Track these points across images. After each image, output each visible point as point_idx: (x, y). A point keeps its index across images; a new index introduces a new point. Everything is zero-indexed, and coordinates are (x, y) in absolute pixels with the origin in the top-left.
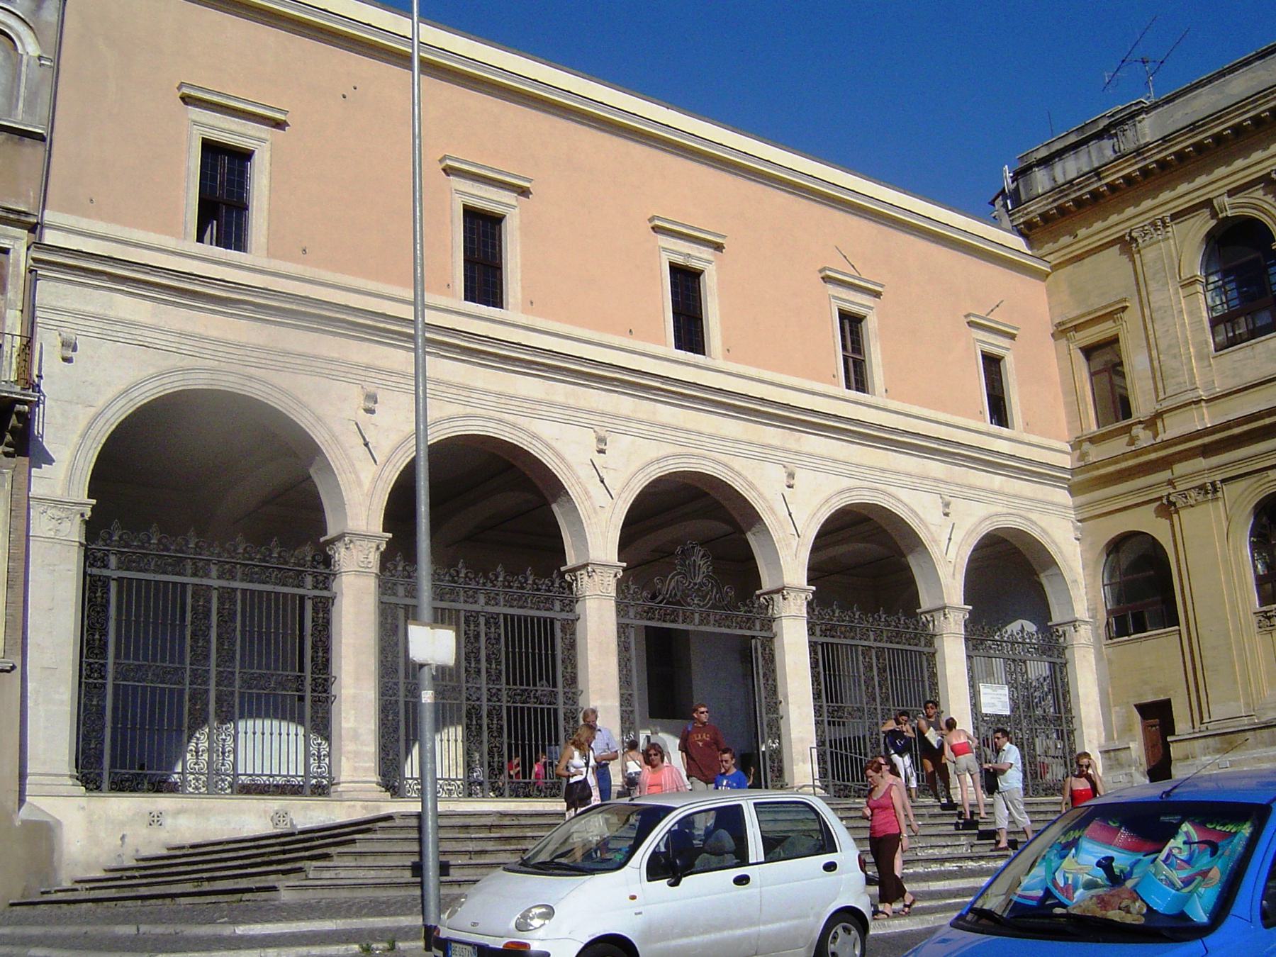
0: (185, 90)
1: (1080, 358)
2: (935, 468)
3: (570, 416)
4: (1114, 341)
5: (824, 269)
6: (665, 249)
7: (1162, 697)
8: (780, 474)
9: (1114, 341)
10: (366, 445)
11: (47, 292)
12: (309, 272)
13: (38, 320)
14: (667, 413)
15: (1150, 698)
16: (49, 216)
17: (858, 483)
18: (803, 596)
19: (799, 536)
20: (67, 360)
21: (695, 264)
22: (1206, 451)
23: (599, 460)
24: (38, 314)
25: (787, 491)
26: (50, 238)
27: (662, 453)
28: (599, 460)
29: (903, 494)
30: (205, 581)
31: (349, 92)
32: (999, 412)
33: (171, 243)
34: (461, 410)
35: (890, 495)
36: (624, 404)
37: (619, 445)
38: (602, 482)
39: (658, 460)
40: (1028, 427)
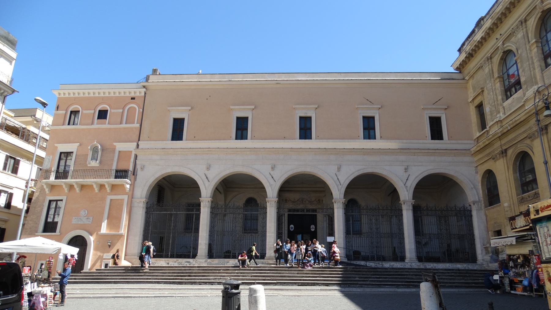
2: (402, 158)
10: (207, 178)
13: (137, 164)
15: (497, 229)
18: (342, 202)
21: (308, 115)
24: (137, 163)
28: (272, 173)
38: (272, 177)
40: (450, 138)
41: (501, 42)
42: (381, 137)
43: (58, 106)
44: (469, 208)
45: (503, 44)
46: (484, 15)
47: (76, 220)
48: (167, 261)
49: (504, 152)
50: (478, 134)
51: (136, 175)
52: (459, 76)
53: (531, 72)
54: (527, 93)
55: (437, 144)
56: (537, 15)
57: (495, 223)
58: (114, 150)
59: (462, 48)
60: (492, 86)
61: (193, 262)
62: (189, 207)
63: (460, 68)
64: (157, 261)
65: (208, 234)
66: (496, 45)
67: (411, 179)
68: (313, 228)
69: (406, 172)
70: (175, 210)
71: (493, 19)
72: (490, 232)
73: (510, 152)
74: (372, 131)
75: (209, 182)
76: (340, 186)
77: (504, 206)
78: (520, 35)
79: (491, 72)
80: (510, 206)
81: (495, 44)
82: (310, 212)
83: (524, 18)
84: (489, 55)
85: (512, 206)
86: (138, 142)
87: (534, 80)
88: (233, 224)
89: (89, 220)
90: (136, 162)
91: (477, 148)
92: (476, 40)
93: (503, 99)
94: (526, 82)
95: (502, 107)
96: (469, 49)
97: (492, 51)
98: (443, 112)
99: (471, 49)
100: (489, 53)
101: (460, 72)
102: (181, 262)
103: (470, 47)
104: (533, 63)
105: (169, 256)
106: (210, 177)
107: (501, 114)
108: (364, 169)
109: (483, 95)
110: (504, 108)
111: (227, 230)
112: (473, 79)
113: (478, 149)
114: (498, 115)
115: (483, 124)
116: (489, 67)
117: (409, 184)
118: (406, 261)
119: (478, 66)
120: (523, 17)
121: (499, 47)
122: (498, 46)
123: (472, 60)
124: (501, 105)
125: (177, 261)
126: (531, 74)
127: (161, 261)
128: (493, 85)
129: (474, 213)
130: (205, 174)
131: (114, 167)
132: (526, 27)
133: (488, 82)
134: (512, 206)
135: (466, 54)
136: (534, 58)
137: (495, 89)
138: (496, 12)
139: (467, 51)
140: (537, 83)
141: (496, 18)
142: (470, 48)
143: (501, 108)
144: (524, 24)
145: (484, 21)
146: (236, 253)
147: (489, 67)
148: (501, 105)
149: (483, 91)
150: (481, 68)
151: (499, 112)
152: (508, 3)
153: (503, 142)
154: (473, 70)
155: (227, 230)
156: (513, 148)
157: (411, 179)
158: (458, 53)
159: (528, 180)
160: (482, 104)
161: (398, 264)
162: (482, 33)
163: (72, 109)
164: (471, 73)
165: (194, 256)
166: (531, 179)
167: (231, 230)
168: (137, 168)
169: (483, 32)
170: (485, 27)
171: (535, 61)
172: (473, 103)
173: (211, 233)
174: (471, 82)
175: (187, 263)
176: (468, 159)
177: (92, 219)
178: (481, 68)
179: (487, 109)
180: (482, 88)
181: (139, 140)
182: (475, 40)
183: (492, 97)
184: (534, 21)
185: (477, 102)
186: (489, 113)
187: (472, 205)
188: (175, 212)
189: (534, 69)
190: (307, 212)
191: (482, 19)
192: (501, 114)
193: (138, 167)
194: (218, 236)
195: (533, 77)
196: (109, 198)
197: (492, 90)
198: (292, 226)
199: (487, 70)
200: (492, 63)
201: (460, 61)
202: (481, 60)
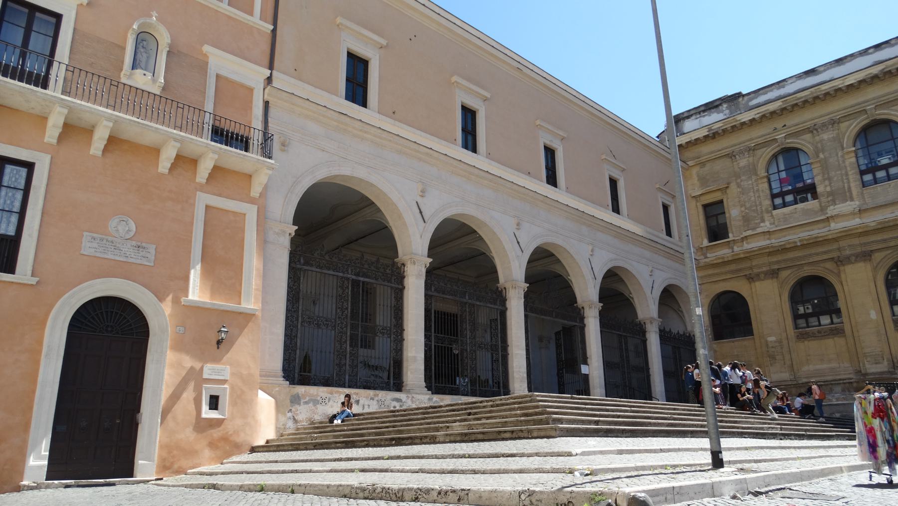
1: (701, 210)
4: (721, 202)
9: (721, 202)
19: (596, 279)
22: (770, 254)
30: (345, 275)
31: (413, 38)
32: (669, 233)
41: (784, 135)
45: (785, 137)
46: (744, 92)
47: (95, 245)
49: (773, 274)
53: (844, 183)
56: (863, 121)
58: (203, 67)
59: (682, 121)
60: (753, 185)
64: (331, 393)
69: (652, 276)
71: (785, 104)
73: (784, 274)
75: (425, 222)
77: (767, 341)
78: (826, 136)
84: (753, 145)
85: (785, 342)
87: (848, 194)
91: (716, 259)
92: (739, 120)
94: (830, 194)
96: (719, 128)
97: (760, 140)
99: (722, 128)
100: (753, 141)
102: (383, 400)
103: (722, 125)
104: (847, 175)
107: (767, 223)
110: (772, 216)
112: (701, 168)
113: (715, 262)
114: (762, 224)
116: (748, 160)
121: (777, 139)
122: (776, 137)
125: (375, 395)
130: (417, 202)
134: (785, 342)
135: (708, 131)
136: (849, 169)
137: (758, 190)
138: (796, 97)
139: (713, 128)
142: (721, 127)
143: (766, 216)
144: (836, 125)
145: (743, 99)
149: (727, 187)
150: (731, 156)
151: (763, 221)
152: (824, 92)
153: (774, 259)
154: (710, 156)
156: (794, 270)
162: (756, 115)
164: (703, 159)
169: (758, 113)
170: (766, 109)
171: (850, 173)
172: (700, 199)
174: (695, 171)
177: (153, 252)
178: (731, 156)
182: (738, 119)
184: (855, 126)
189: (849, 182)
191: (739, 95)
192: (767, 223)
195: (847, 191)
196: (204, 199)
197: (752, 190)
200: (753, 156)
201: (691, 138)
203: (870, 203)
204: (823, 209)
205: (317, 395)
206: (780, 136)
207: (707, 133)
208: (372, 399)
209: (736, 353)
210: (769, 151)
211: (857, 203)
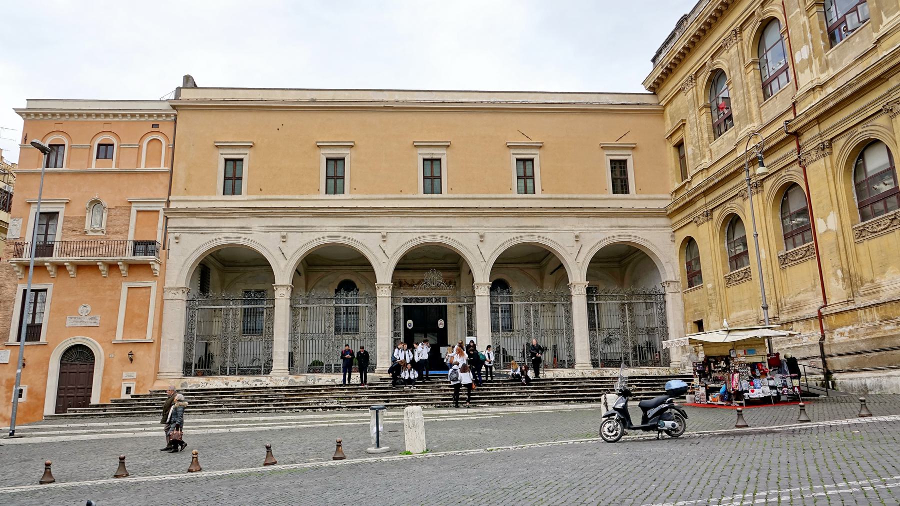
0: (216, 144)
3: (370, 230)
5: (507, 143)
6: (420, 154)
7: (701, 319)
8: (476, 236)
11: (171, 223)
12: (263, 197)
14: (417, 221)
15: (697, 319)
16: (171, 198)
17: (522, 234)
18: (486, 286)
20: (177, 243)
23: (383, 244)
25: (480, 245)
26: (172, 205)
27: (415, 237)
29: (550, 236)
33: (213, 198)
34: (322, 235)
35: (540, 237)
36: (397, 221)
37: (393, 238)
39: (411, 241)
40: (639, 190)
41: (710, 57)
42: (543, 190)
43: (26, 137)
44: (662, 291)
46: (688, 13)
47: (72, 321)
48: (225, 381)
50: (677, 186)
51: (169, 249)
52: (651, 100)
54: (740, 133)
55: (621, 201)
57: (695, 311)
61: (265, 381)
62: (257, 297)
63: (655, 87)
64: (209, 380)
65: (287, 339)
66: (702, 60)
67: (585, 251)
68: (441, 324)
70: (233, 303)
71: (700, 22)
72: (688, 323)
74: (529, 182)
76: (483, 264)
77: (707, 288)
78: (733, 50)
79: (695, 98)
80: (714, 288)
81: (701, 58)
82: (440, 302)
83: (739, 26)
86: (169, 197)
88: (325, 322)
89: (94, 321)
90: (166, 228)
93: (709, 139)
95: (708, 149)
96: (667, 62)
97: (697, 67)
98: (629, 152)
101: (654, 94)
104: (748, 92)
105: (228, 373)
106: (289, 253)
108: (519, 237)
109: (684, 129)
110: (710, 150)
111: (317, 332)
115: (684, 173)
116: (693, 91)
117: (581, 258)
118: (577, 367)
119: (679, 87)
120: (737, 25)
123: (671, 77)
124: (707, 146)
126: (745, 108)
127: (216, 381)
128: (697, 116)
129: (668, 298)
131: (131, 237)
132: (742, 40)
133: (691, 112)
134: (717, 289)
135: (662, 68)
136: (750, 85)
140: (752, 121)
141: (703, 22)
144: (738, 35)
146: (331, 365)
147: (693, 91)
148: (707, 146)
149: (684, 124)
151: (704, 157)
153: (710, 198)
155: (317, 332)
157: (585, 251)
158: (652, 63)
159: (738, 252)
160: (683, 143)
161: (565, 372)
162: (684, 41)
163: (51, 141)
164: (669, 97)
165: (268, 372)
166: (742, 251)
167: (323, 332)
168: (169, 238)
169: (686, 39)
173: (292, 337)
174: (668, 109)
175: (256, 383)
176: (663, 221)
177: (99, 319)
179: (689, 150)
180: (682, 120)
181: (170, 194)
183: (696, 134)
185: (676, 139)
186: (692, 157)
187: (666, 286)
188: (234, 307)
189: (750, 100)
190: (435, 302)
191: (685, 18)
193: (171, 237)
194: (302, 341)
198: (410, 322)
199: (690, 94)
202: (682, 79)
203: (766, 121)
204: (737, 134)
205: (198, 382)
206: (707, 58)
207: (662, 70)
208: (238, 381)
209: (696, 302)
210: (703, 79)
211: (756, 124)
